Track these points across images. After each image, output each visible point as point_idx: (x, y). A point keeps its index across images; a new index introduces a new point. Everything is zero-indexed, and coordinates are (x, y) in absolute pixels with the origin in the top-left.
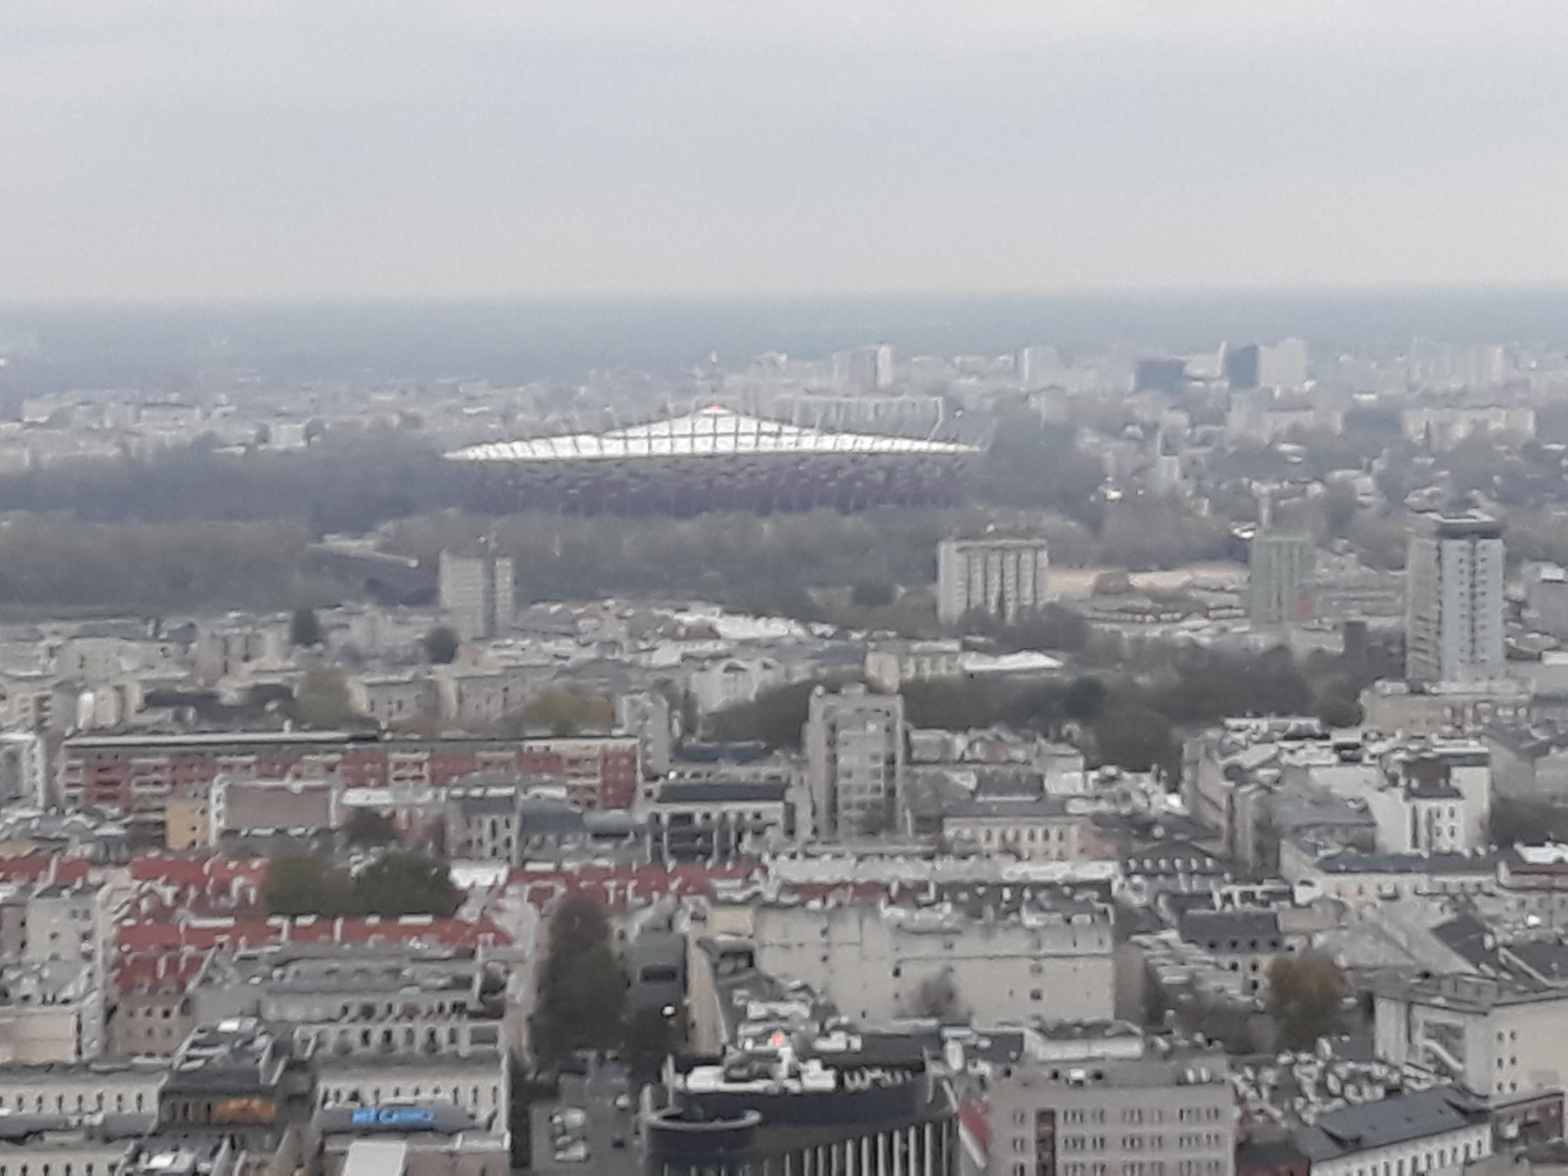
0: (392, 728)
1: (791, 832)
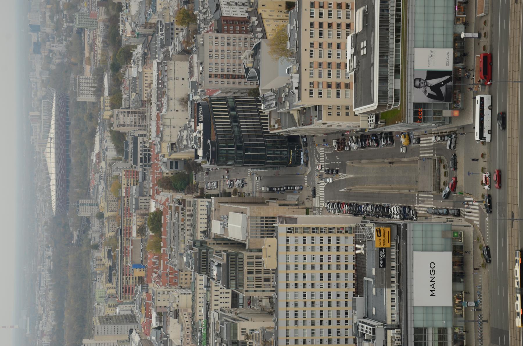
0: (119, 226)
1: (145, 136)
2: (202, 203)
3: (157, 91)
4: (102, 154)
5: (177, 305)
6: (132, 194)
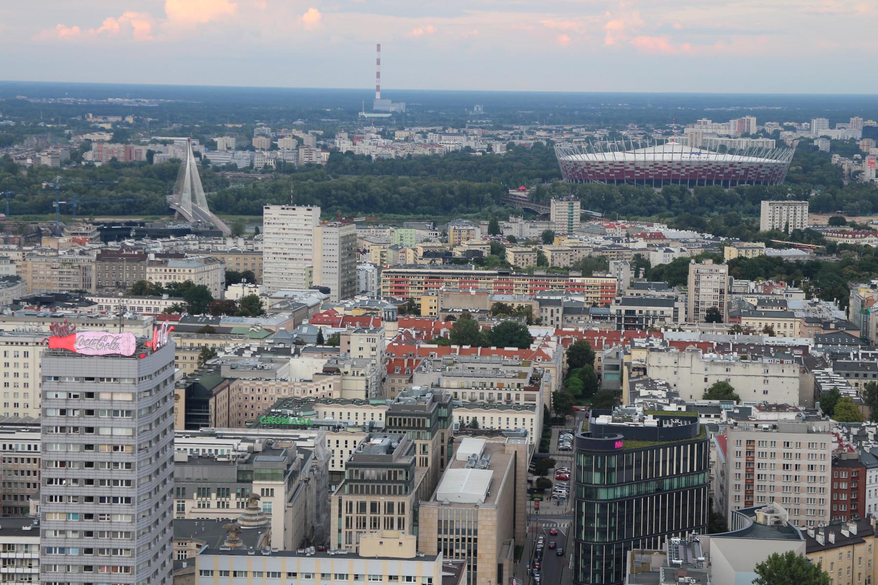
1: (675, 319)
2: (528, 422)
3: (753, 345)
4: (661, 242)
5: (346, 373)
6: (571, 295)
